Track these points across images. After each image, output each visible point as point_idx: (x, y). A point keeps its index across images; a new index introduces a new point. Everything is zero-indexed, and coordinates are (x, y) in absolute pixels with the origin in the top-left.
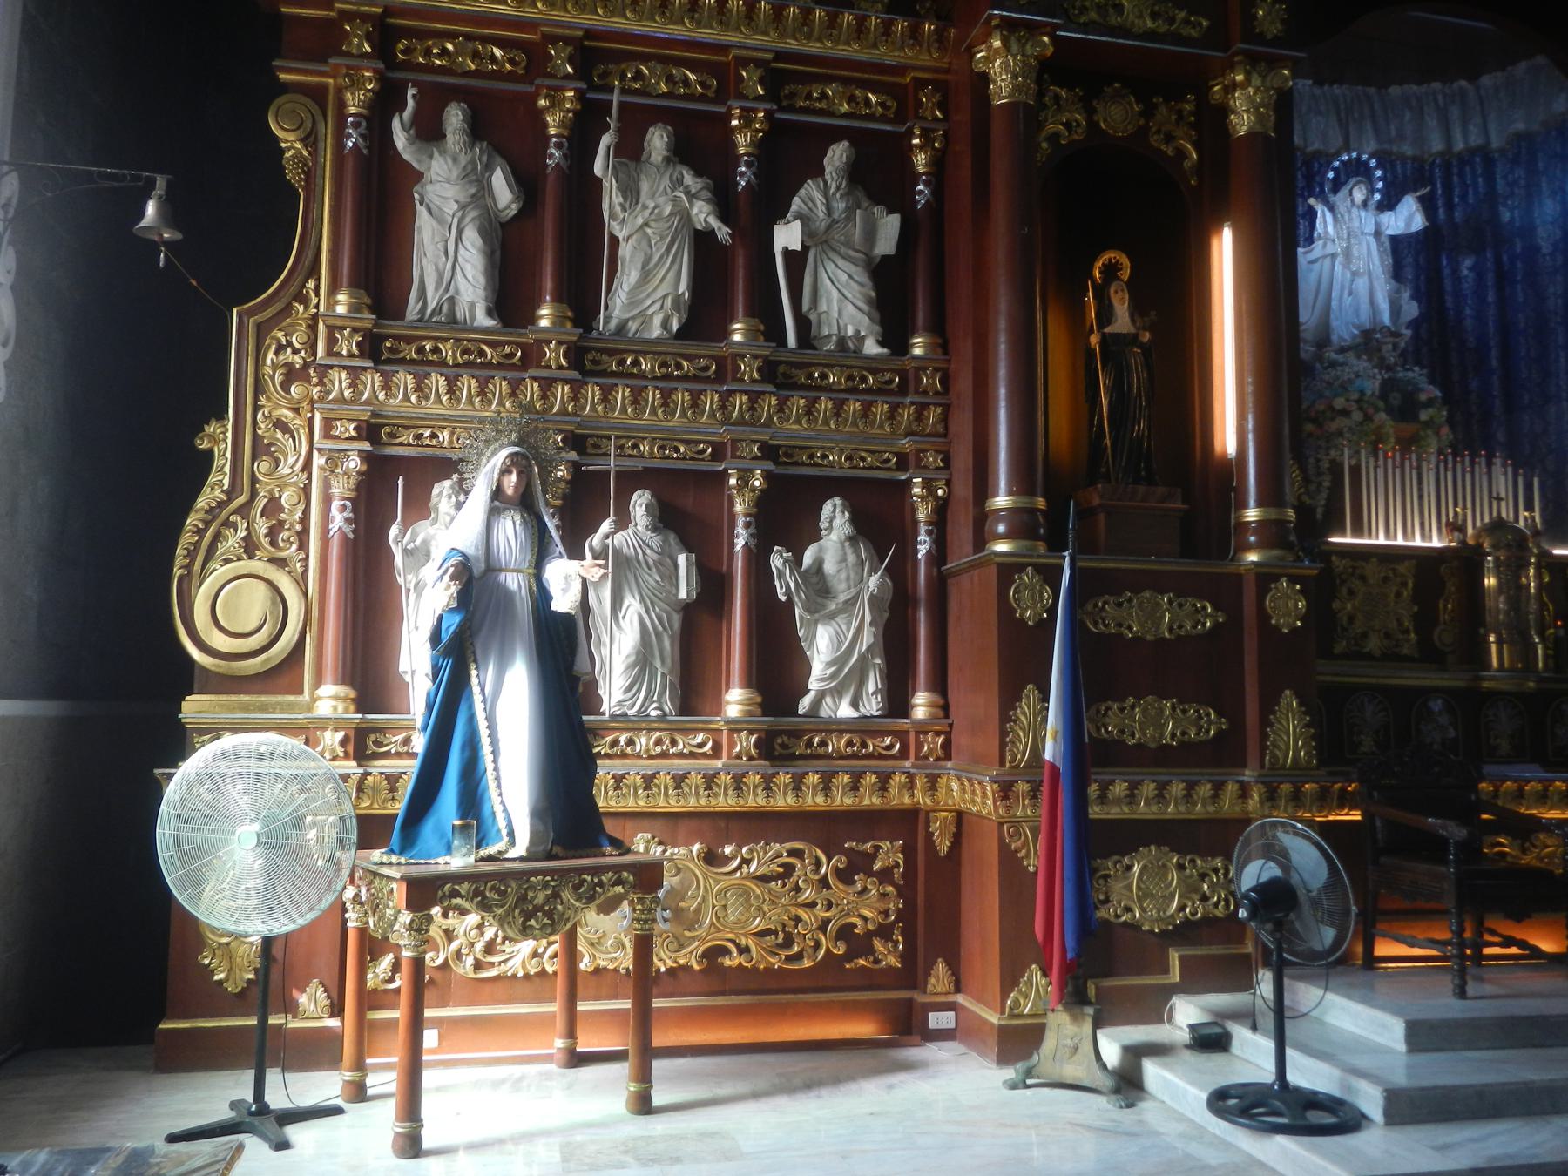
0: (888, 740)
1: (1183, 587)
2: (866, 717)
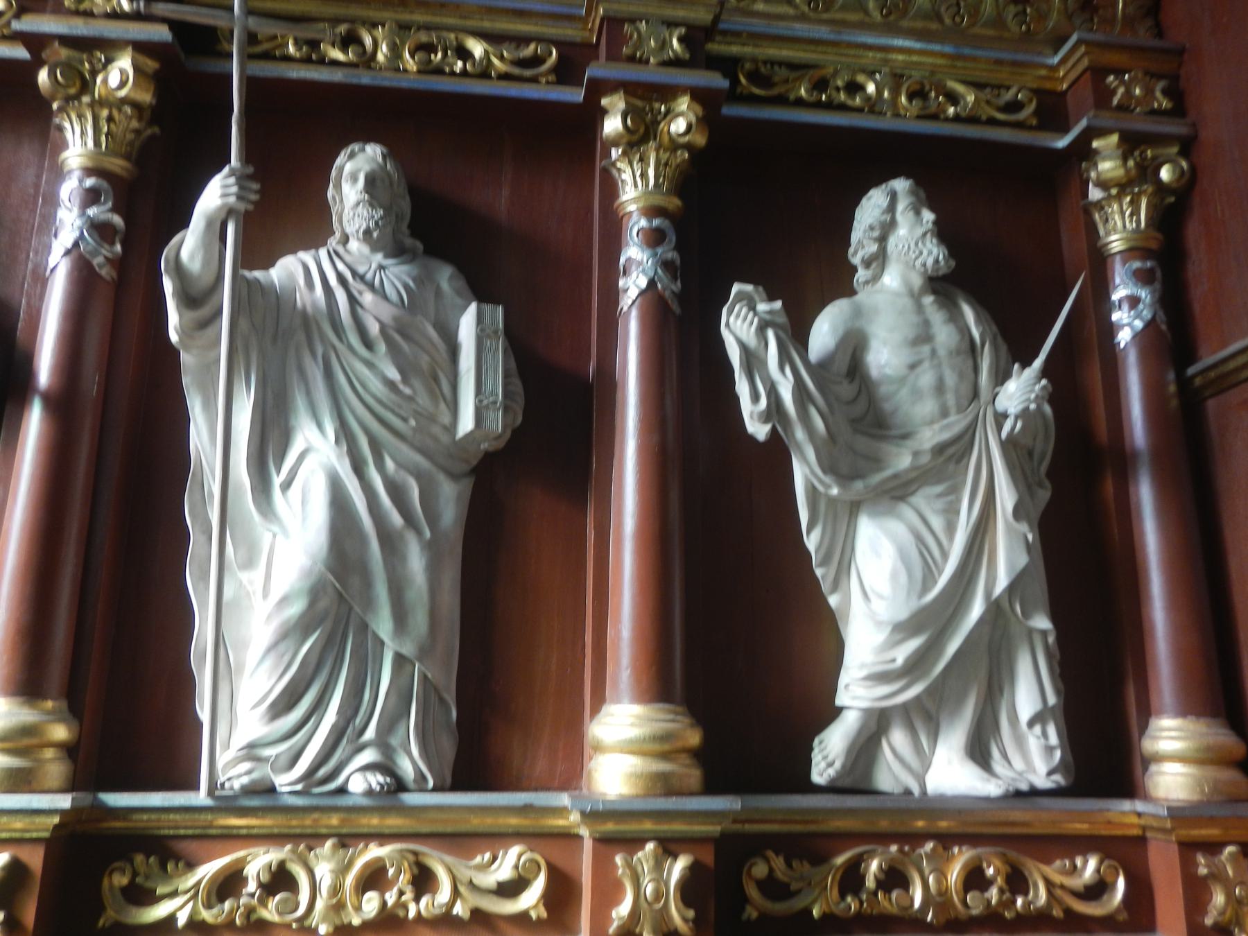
0: (1090, 867)
2: (1018, 794)
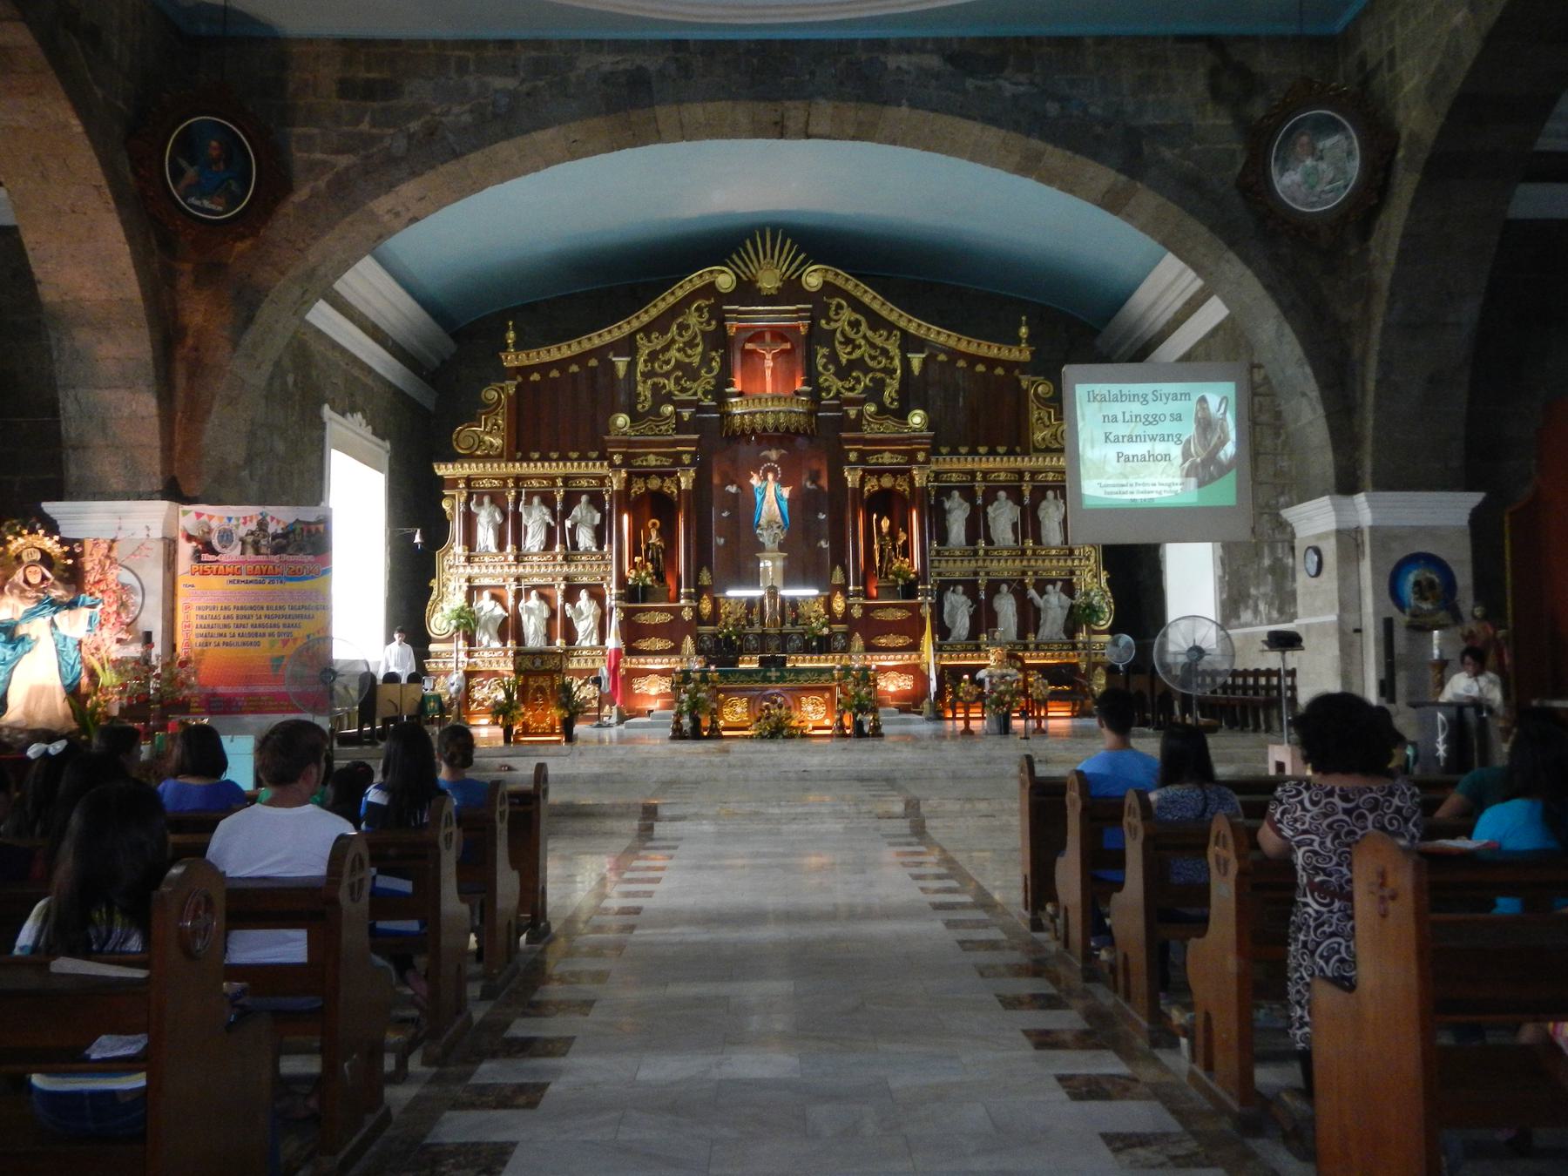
1: (662, 610)
